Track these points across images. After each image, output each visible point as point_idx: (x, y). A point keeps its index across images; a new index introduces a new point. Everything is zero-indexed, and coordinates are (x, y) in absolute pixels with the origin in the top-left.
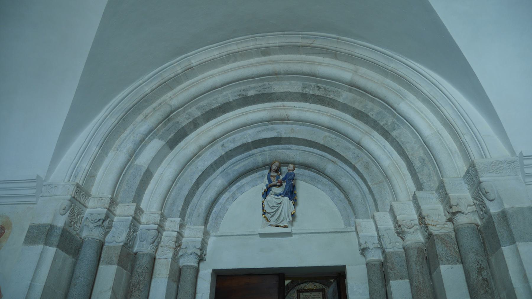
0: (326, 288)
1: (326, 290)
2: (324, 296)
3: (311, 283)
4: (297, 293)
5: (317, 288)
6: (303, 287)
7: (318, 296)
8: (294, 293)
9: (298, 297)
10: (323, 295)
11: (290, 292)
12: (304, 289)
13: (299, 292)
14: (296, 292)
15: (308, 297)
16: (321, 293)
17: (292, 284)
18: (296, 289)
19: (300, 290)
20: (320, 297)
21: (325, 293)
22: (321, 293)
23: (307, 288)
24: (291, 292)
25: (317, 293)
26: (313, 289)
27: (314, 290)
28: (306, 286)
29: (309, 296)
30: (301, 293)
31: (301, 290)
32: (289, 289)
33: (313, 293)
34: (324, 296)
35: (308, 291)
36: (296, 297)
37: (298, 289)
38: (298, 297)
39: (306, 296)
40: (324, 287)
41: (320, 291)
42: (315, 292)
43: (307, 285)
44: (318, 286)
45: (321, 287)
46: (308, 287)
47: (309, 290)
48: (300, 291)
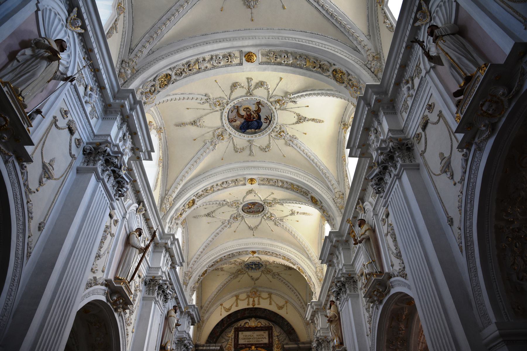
0: (274, 326)
1: (274, 329)
3: (253, 319)
4: (235, 332)
5: (262, 326)
6: (242, 325)
7: (263, 336)
8: (231, 331)
9: (236, 337)
11: (226, 331)
12: (245, 326)
13: (238, 330)
14: (233, 330)
15: (250, 337)
16: (267, 332)
17: (228, 320)
18: (233, 327)
19: (239, 328)
21: (272, 332)
22: (267, 332)
24: (228, 330)
26: (257, 327)
27: (257, 328)
28: (247, 323)
29: (250, 336)
30: (240, 332)
31: (241, 328)
32: (223, 327)
33: (256, 332)
34: (271, 336)
35: (250, 329)
36: (233, 337)
37: (236, 327)
38: (236, 337)
39: (246, 336)
40: (271, 324)
41: (266, 330)
42: (259, 330)
43: (248, 321)
44: (263, 323)
45: (268, 325)
46: (250, 324)
48: (239, 329)
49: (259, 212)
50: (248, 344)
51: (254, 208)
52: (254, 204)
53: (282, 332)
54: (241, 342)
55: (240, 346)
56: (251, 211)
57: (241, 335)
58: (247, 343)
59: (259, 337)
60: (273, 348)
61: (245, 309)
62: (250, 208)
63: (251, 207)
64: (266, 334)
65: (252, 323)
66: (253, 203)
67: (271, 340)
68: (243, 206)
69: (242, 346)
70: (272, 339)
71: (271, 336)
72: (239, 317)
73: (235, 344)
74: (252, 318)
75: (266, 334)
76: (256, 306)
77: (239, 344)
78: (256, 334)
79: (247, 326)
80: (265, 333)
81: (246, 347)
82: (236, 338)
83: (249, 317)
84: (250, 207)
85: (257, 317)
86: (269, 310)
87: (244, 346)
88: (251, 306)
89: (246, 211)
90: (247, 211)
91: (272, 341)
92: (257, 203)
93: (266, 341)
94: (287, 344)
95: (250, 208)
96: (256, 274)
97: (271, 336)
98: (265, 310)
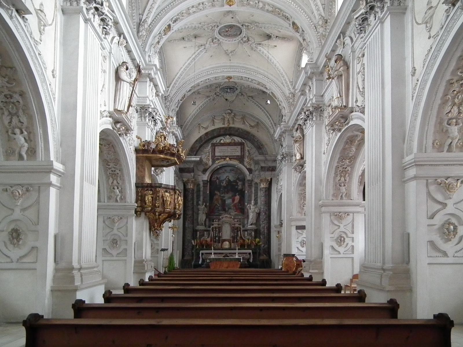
1: (245, 144)
2: (242, 150)
3: (228, 136)
5: (235, 142)
10: (241, 149)
15: (224, 151)
20: (238, 151)
22: (239, 147)
23: (223, 142)
25: (235, 147)
26: (231, 143)
29: (225, 150)
34: (242, 150)
41: (239, 145)
42: (232, 145)
43: (223, 138)
44: (237, 139)
45: (240, 141)
47: (225, 143)
49: (236, 35)
50: (223, 156)
51: (232, 32)
52: (231, 27)
53: (252, 146)
54: (217, 154)
55: (216, 157)
56: (228, 35)
57: (217, 149)
58: (222, 155)
59: (233, 151)
60: (244, 159)
61: (221, 128)
62: (227, 31)
63: (228, 30)
64: (239, 148)
65: (227, 139)
66: (230, 25)
67: (242, 153)
68: (220, 29)
69: (218, 157)
70: (244, 152)
71: (243, 150)
72: (215, 135)
73: (212, 156)
74: (227, 135)
75: (239, 148)
76: (231, 125)
77: (216, 156)
78: (230, 148)
79: (222, 142)
80: (238, 147)
81: (221, 159)
82: (214, 151)
83: (224, 135)
84: (227, 29)
85: (230, 135)
86: (242, 129)
87: (220, 157)
88: (226, 126)
89: (223, 35)
90: (224, 35)
91: (244, 154)
92: (234, 25)
93: (239, 154)
94: (256, 156)
95: (227, 31)
96: (230, 96)
97: (243, 150)
98: (239, 129)
